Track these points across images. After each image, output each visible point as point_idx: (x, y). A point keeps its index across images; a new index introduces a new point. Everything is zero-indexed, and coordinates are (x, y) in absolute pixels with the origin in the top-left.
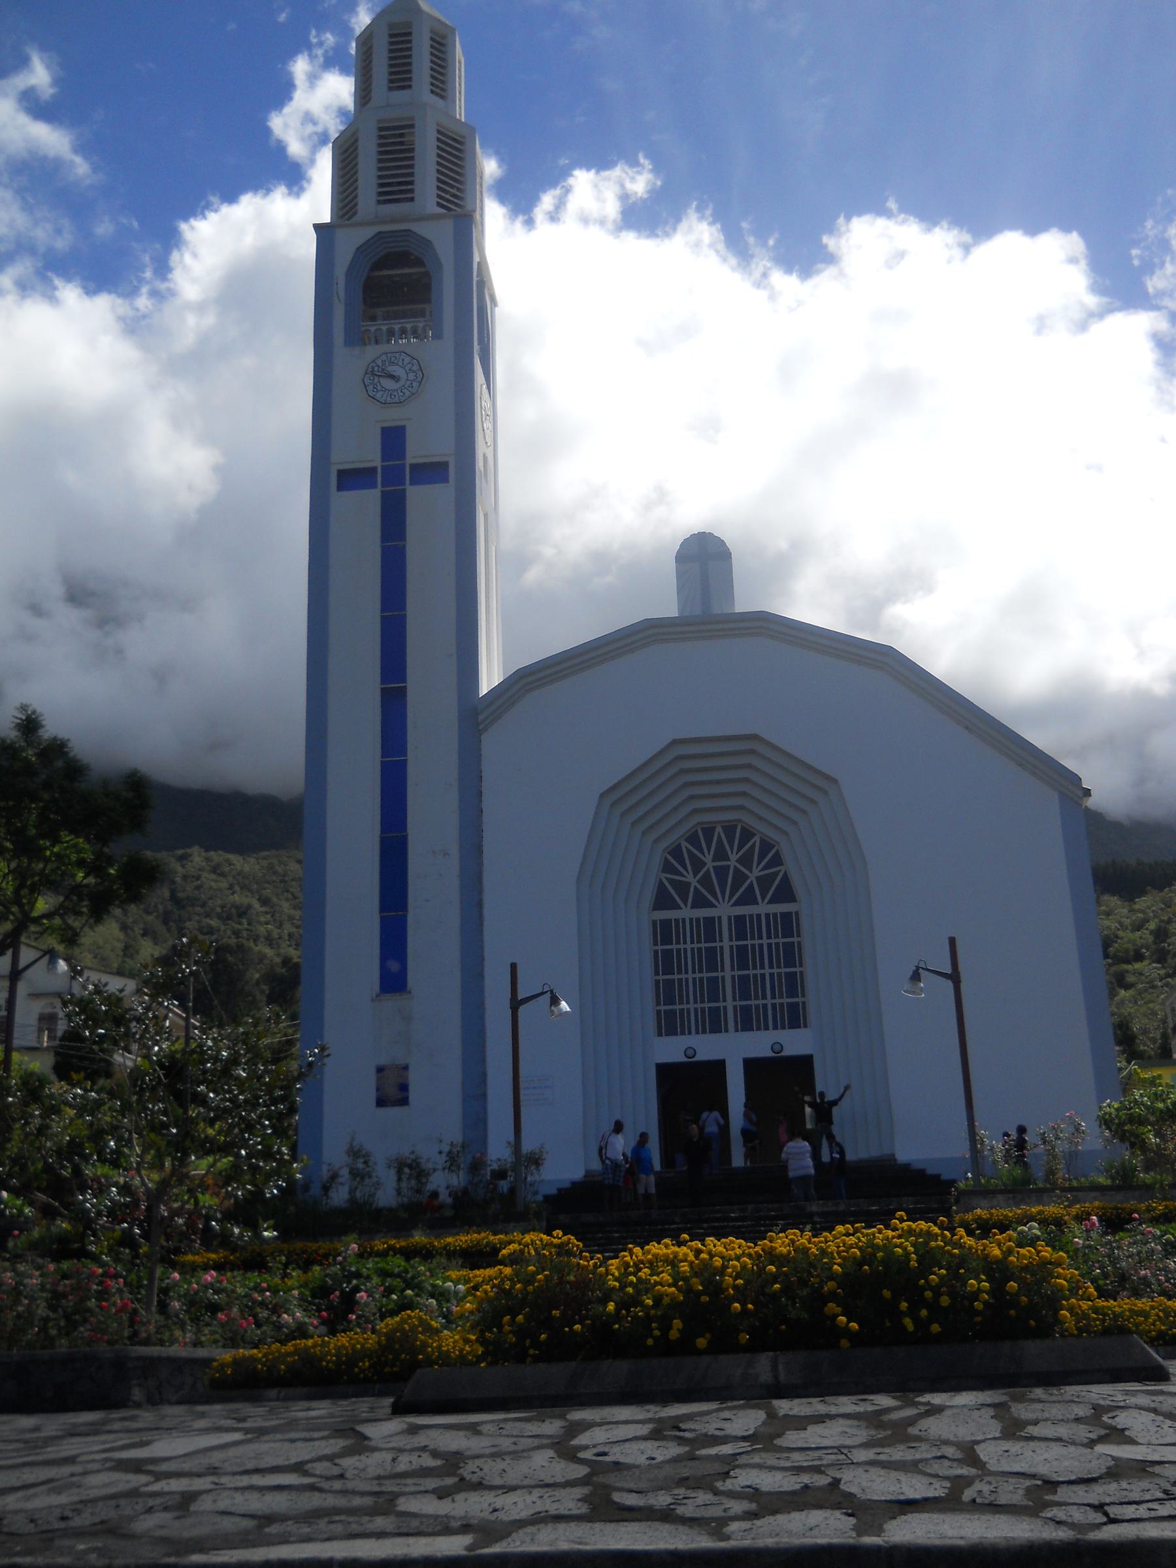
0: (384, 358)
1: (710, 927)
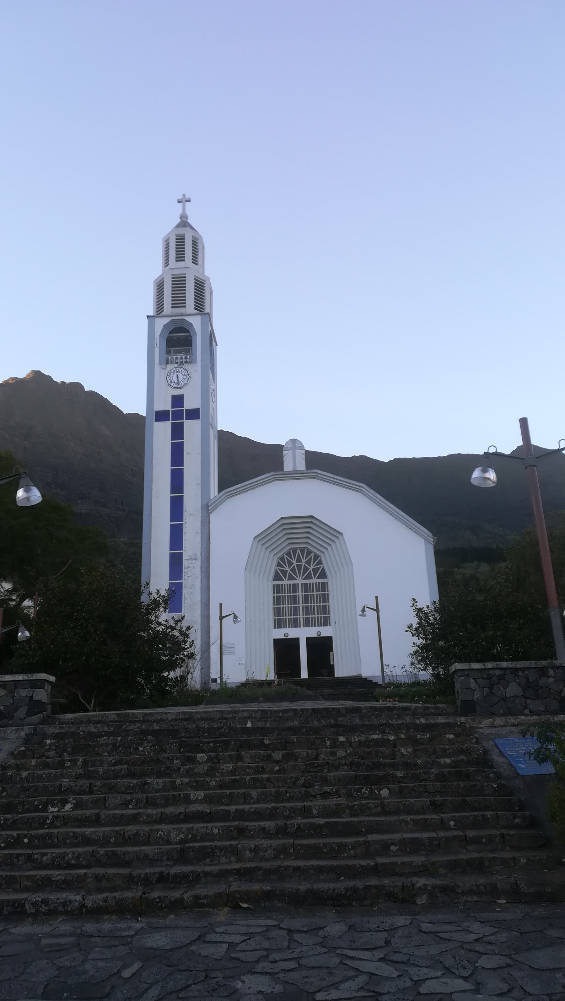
0: (174, 369)
1: (294, 588)
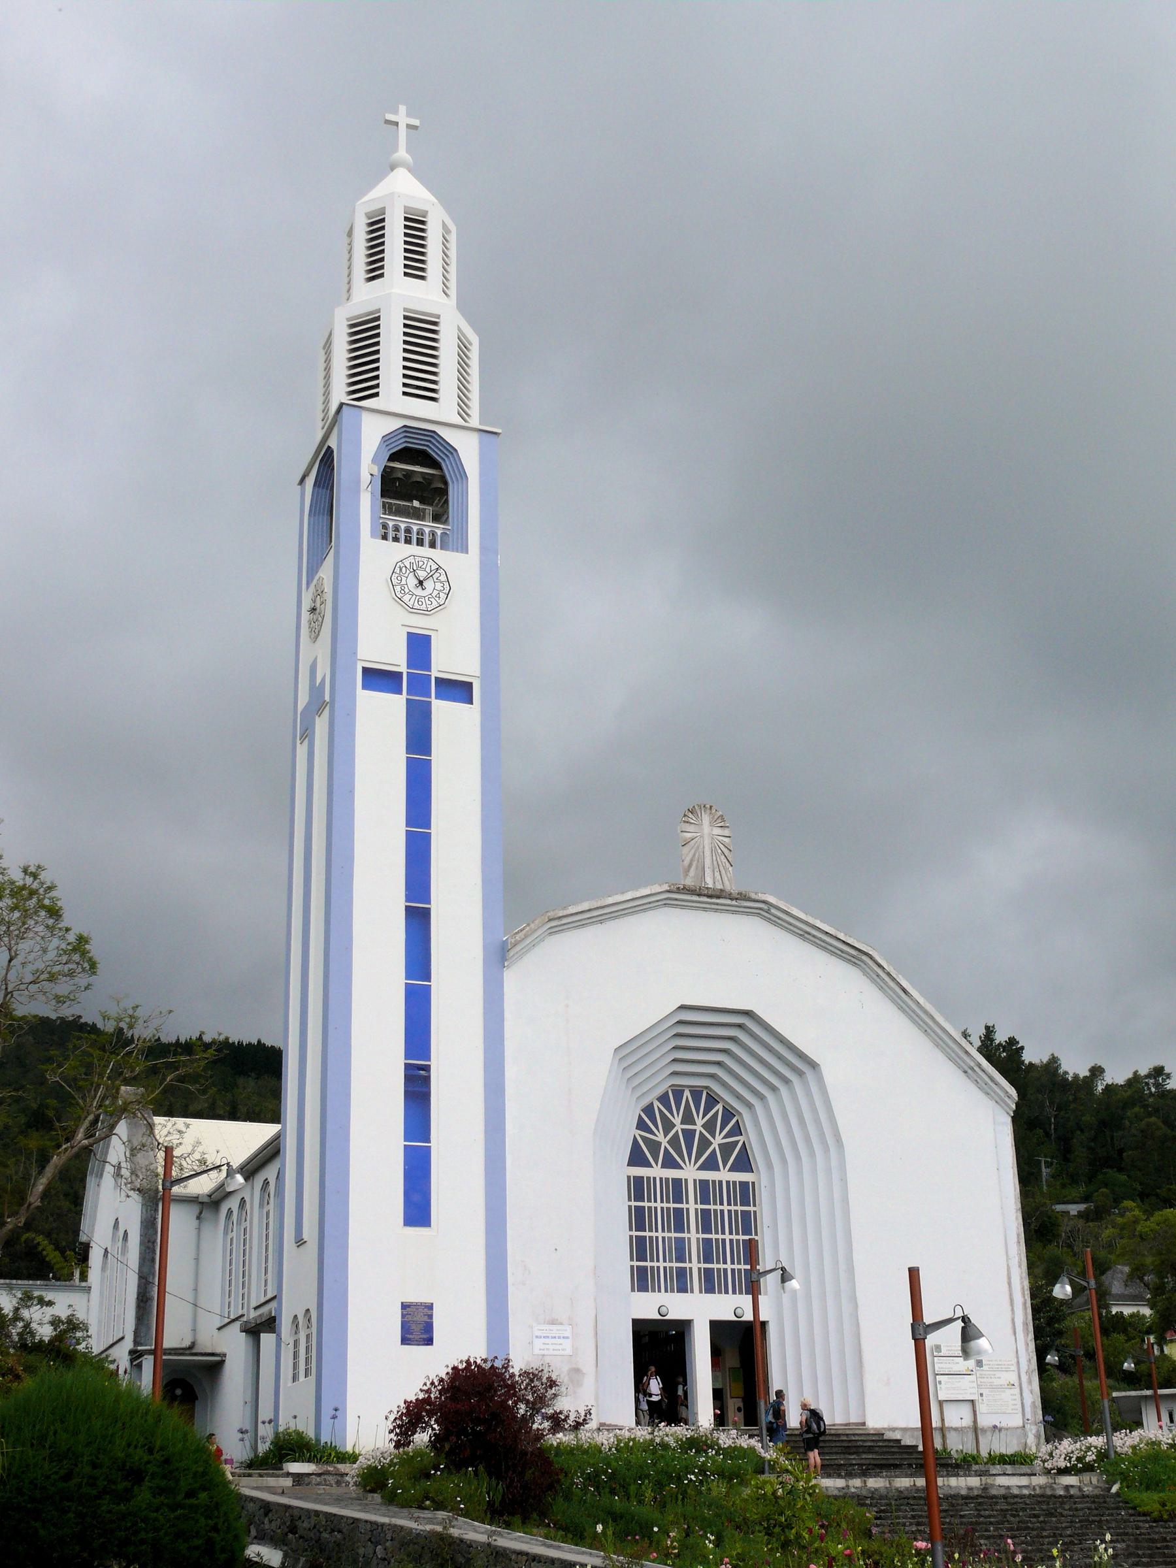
1: (677, 1189)
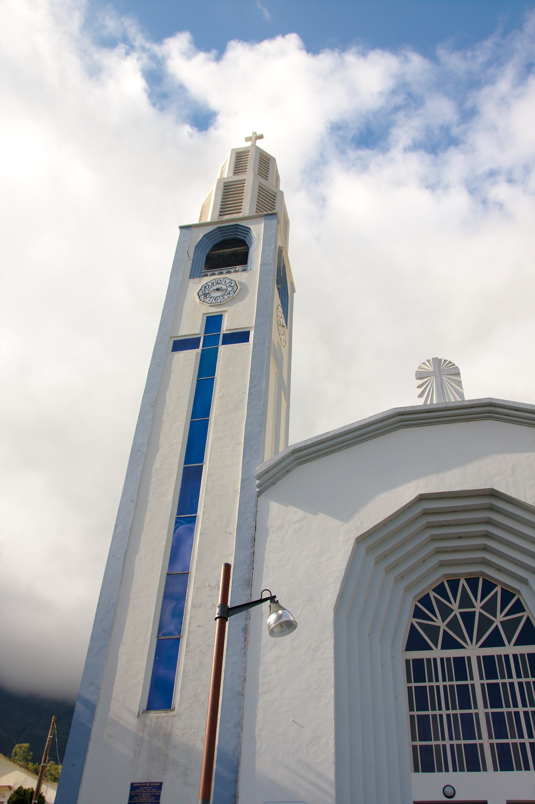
1: (460, 667)
